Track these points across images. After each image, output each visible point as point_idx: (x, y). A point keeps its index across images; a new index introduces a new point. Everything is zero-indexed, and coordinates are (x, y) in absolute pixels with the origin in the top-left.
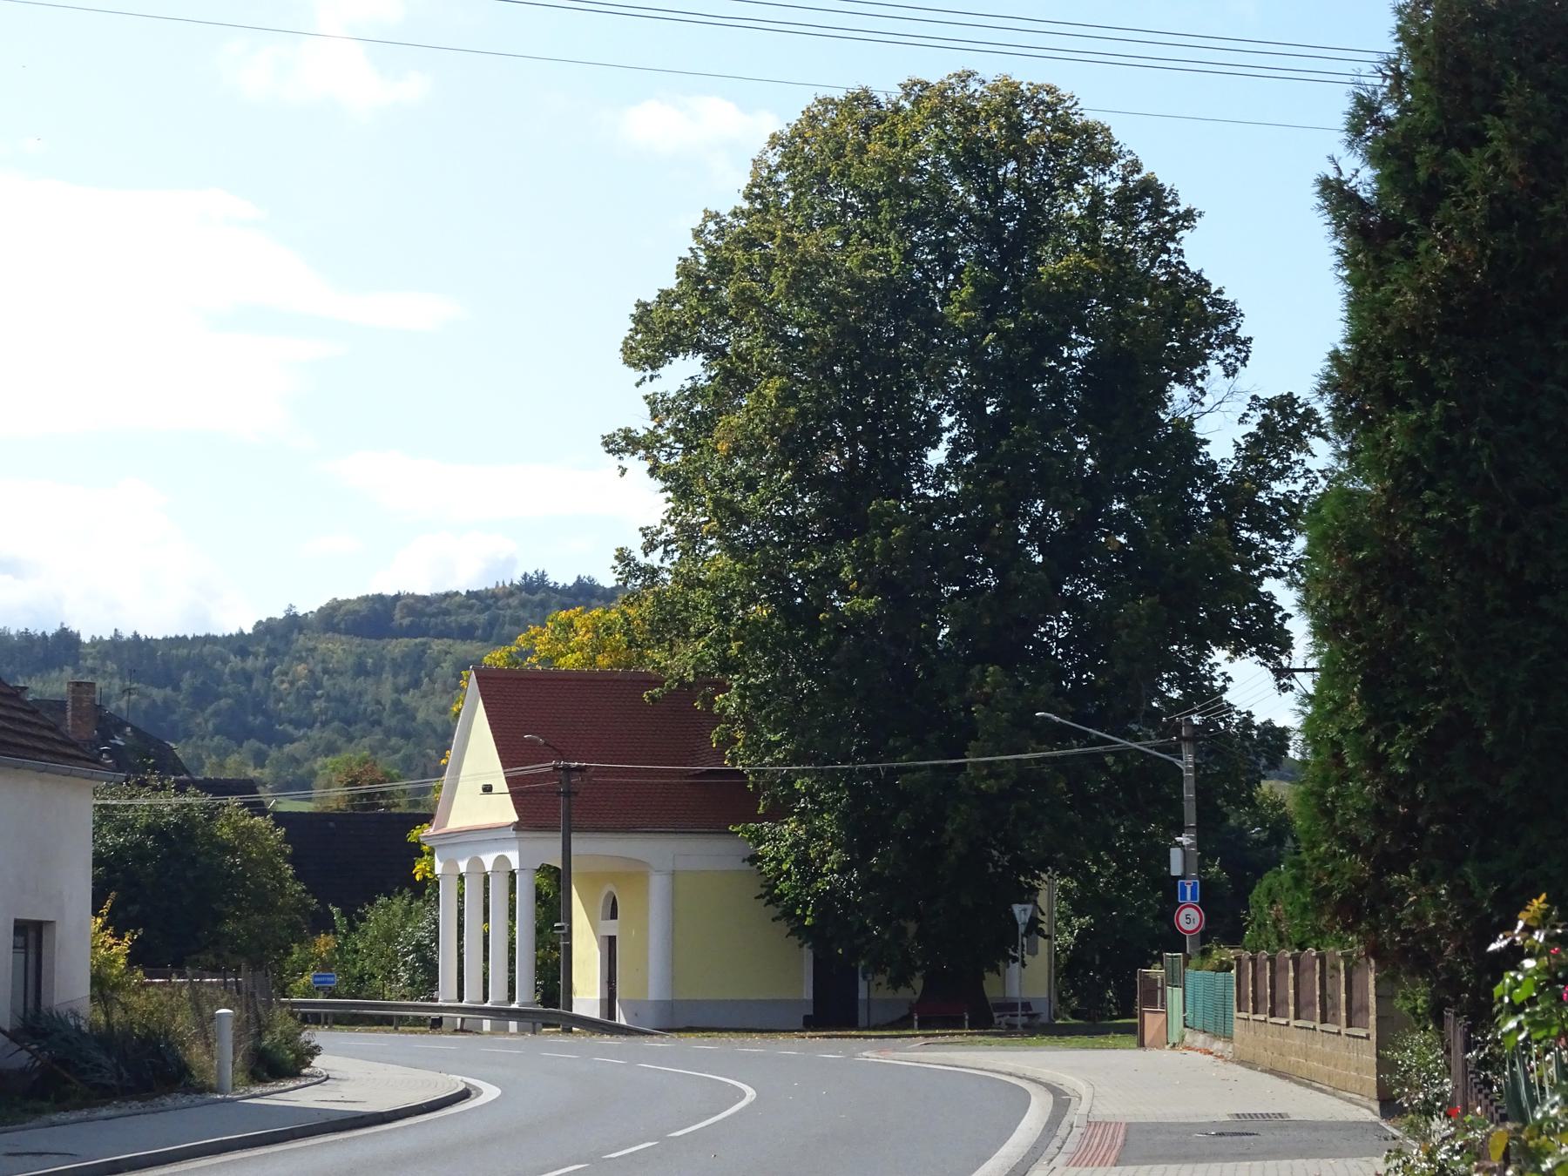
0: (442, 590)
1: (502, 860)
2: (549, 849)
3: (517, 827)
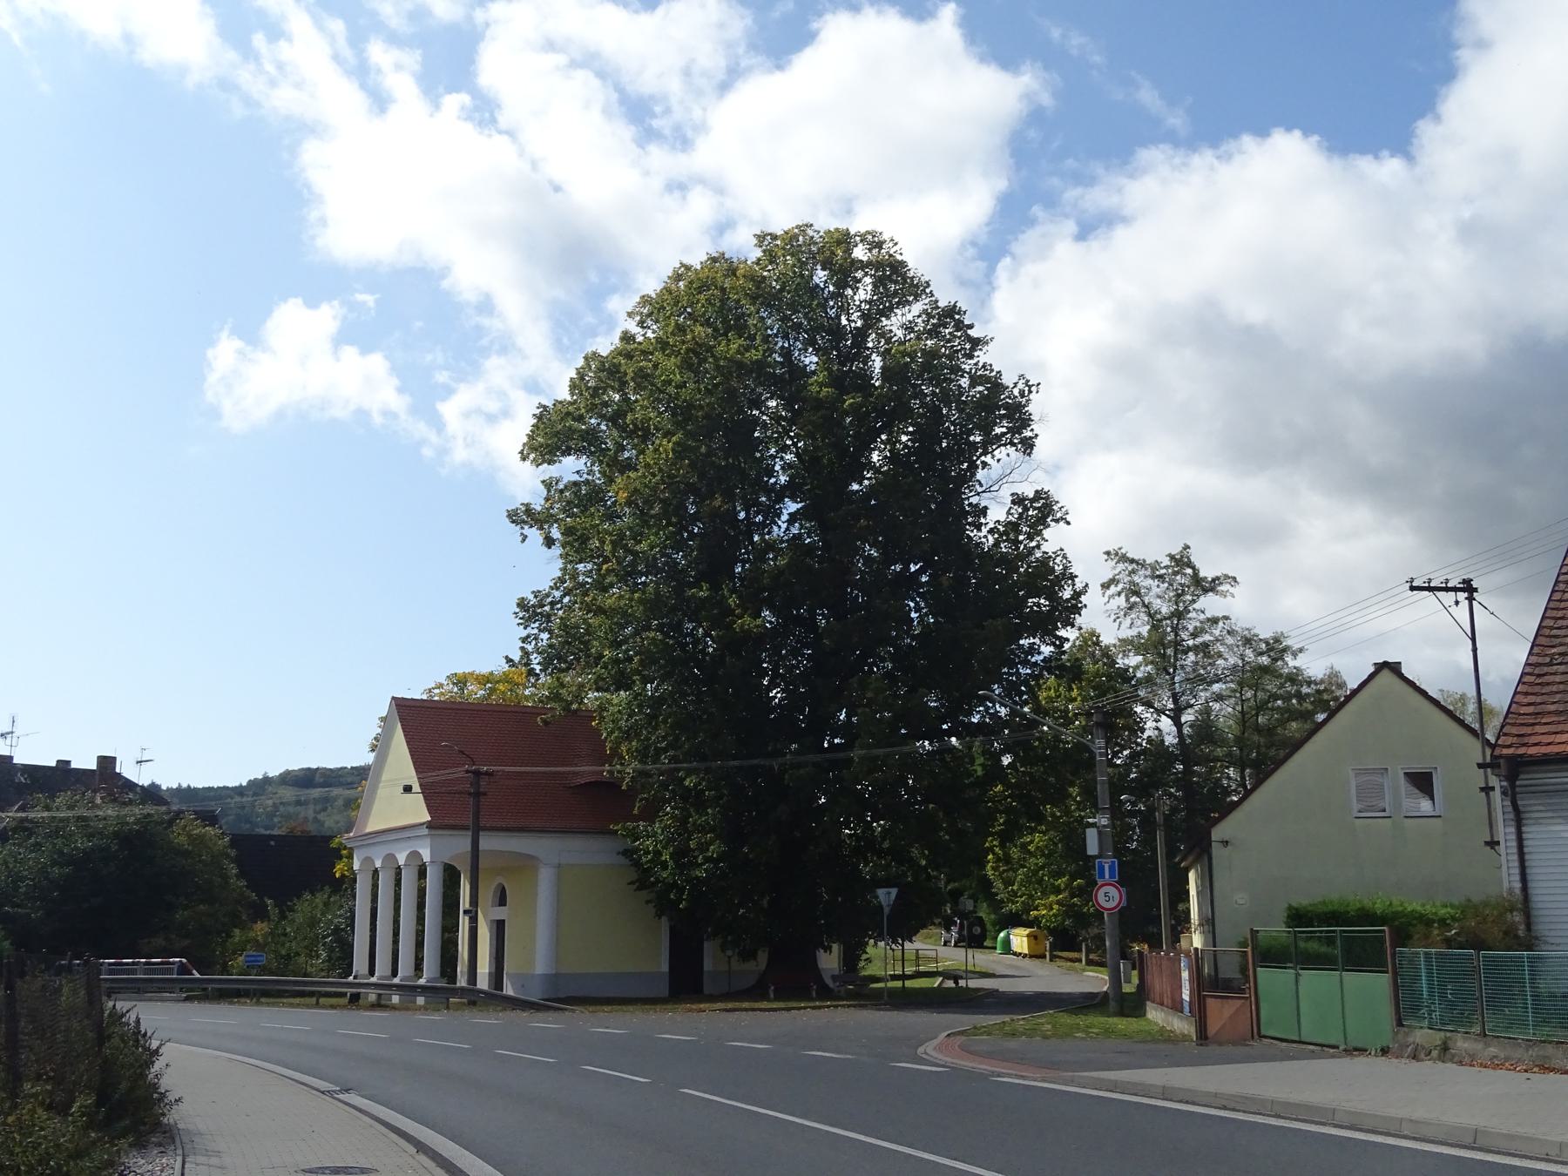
0: (339, 766)
1: (415, 855)
2: (457, 846)
3: (430, 825)
